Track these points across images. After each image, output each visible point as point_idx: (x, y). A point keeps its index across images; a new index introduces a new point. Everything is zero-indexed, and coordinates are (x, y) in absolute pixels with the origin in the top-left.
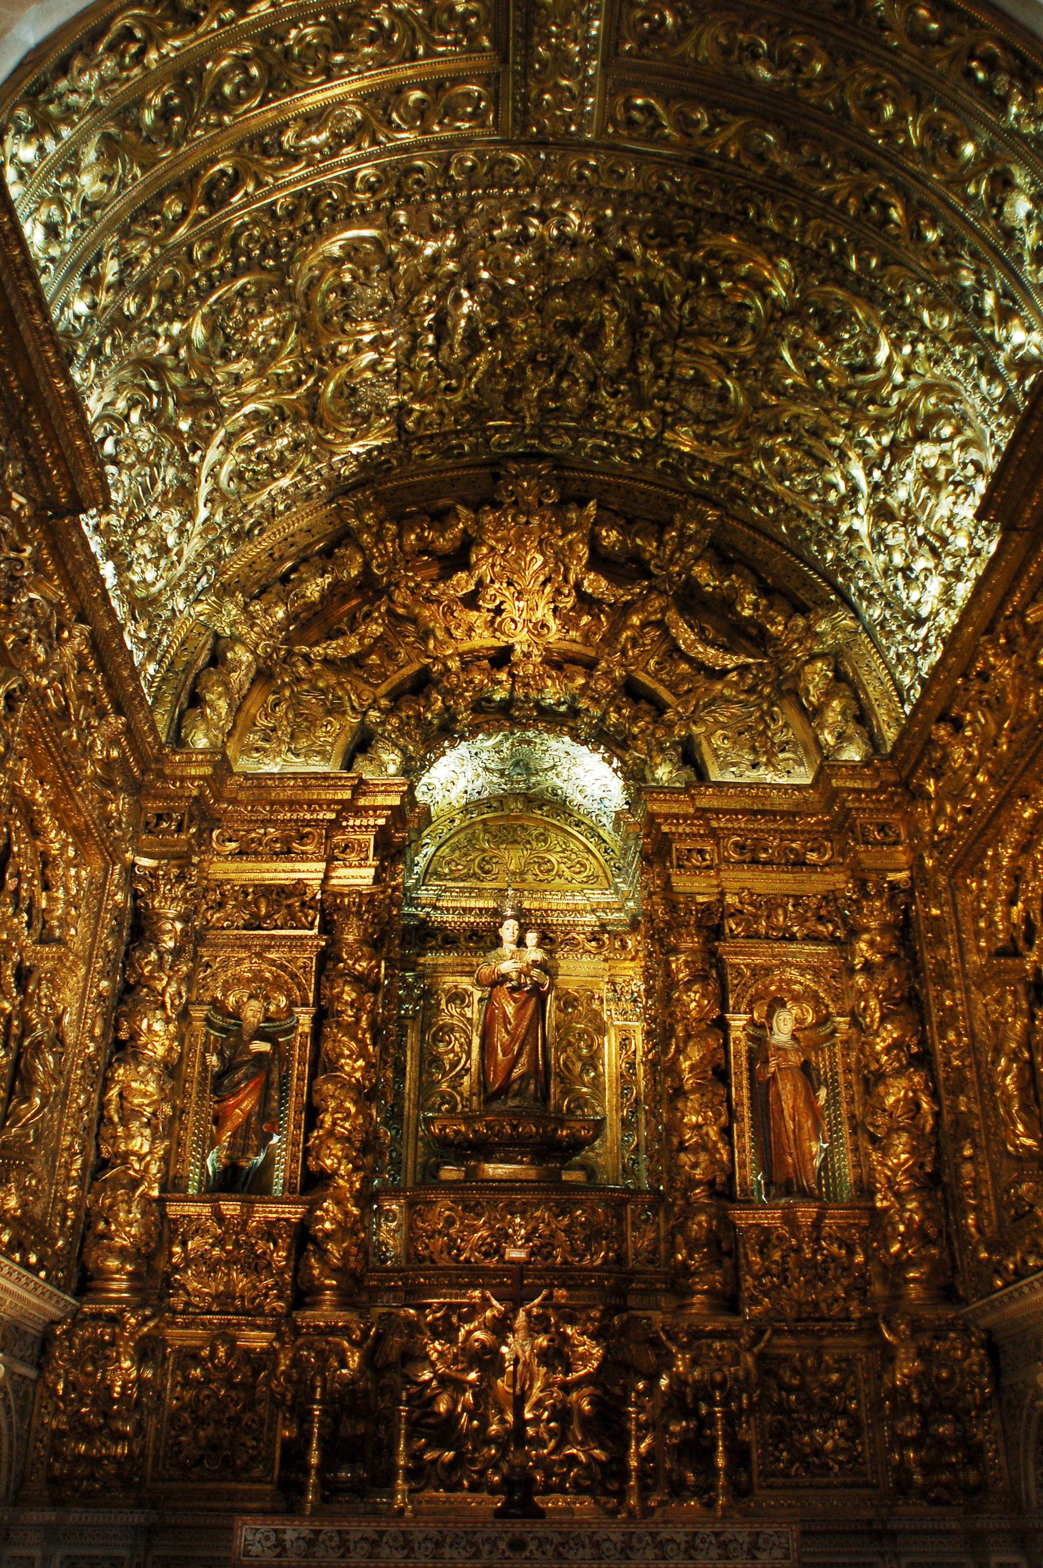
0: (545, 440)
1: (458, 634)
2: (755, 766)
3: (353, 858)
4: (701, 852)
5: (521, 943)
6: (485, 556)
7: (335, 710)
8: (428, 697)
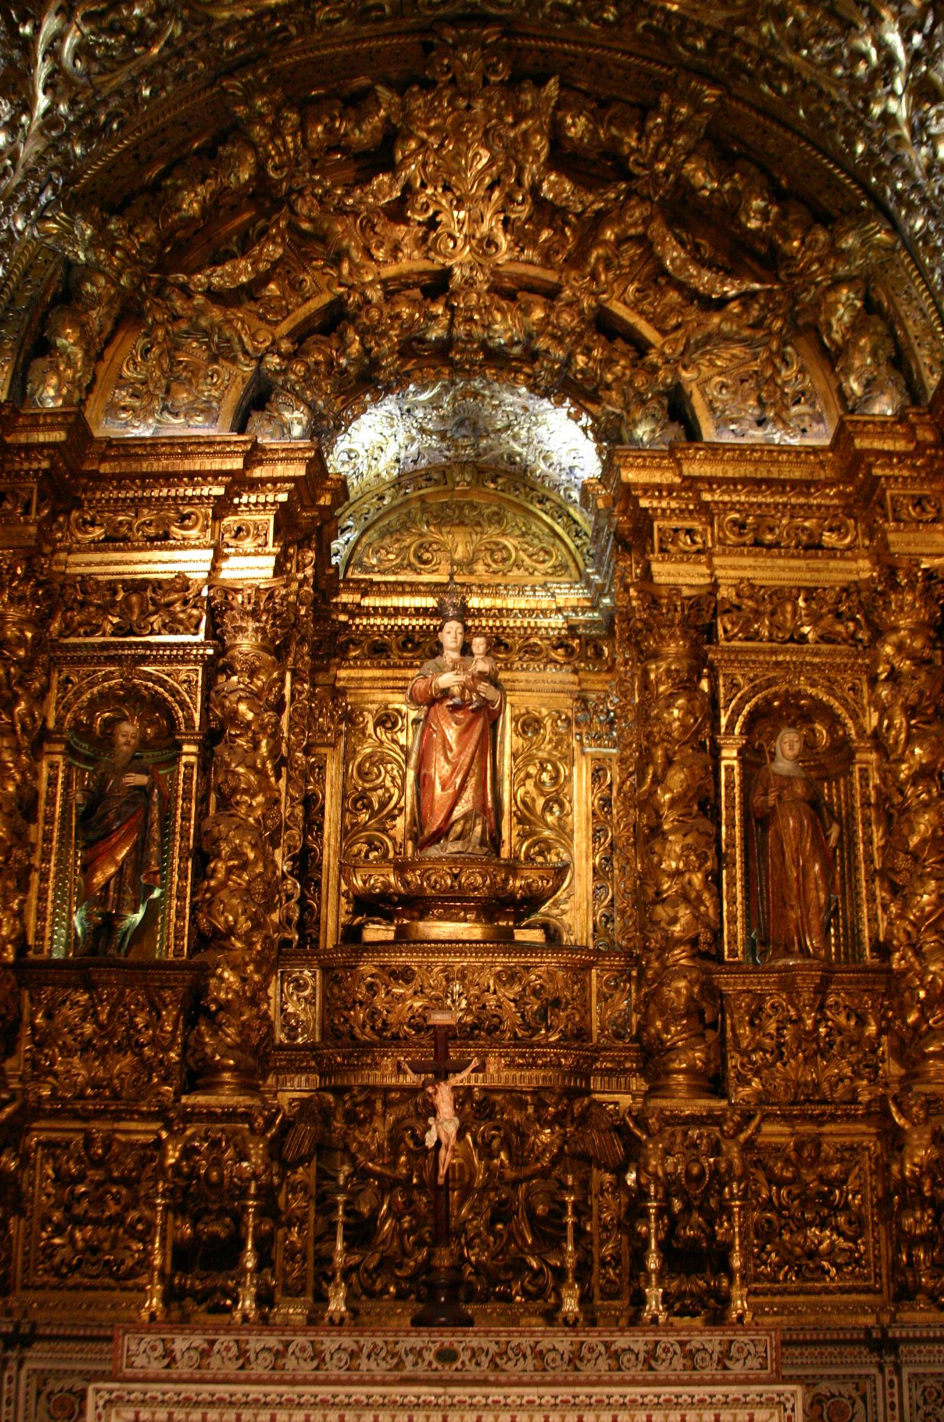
1: (380, 254)
2: (761, 423)
3: (248, 544)
4: (690, 532)
5: (466, 650)
6: (414, 153)
7: (222, 353)
8: (342, 337)
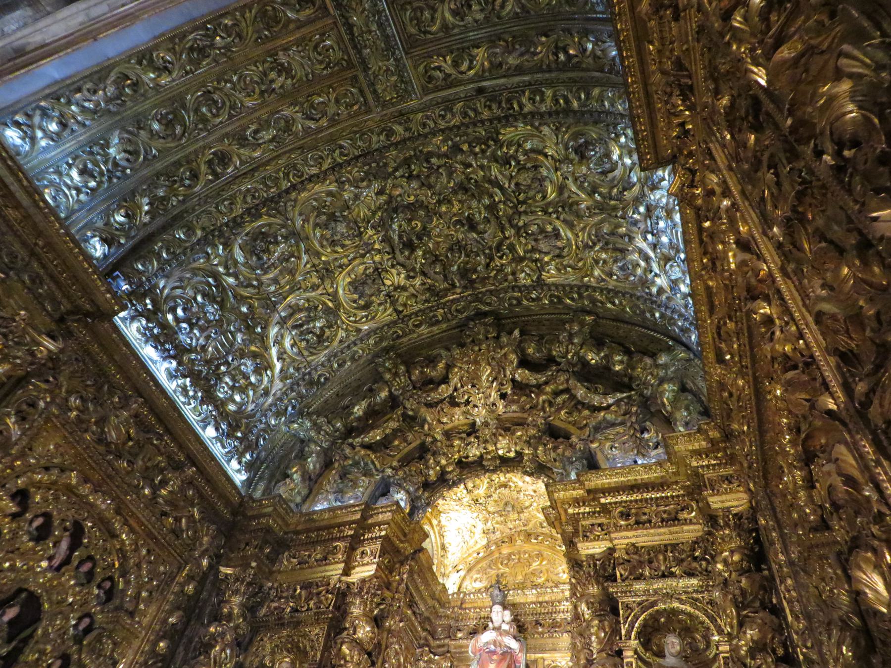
4: (600, 525)
7: (367, 473)
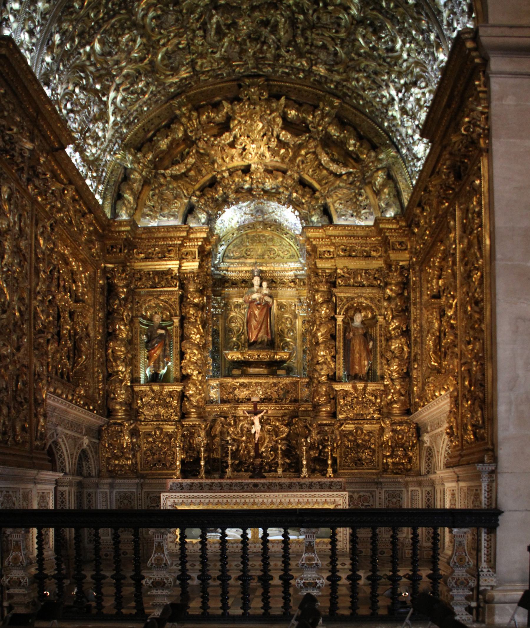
0: (261, 69)
1: (227, 160)
6: (237, 125)
8: (216, 189)
